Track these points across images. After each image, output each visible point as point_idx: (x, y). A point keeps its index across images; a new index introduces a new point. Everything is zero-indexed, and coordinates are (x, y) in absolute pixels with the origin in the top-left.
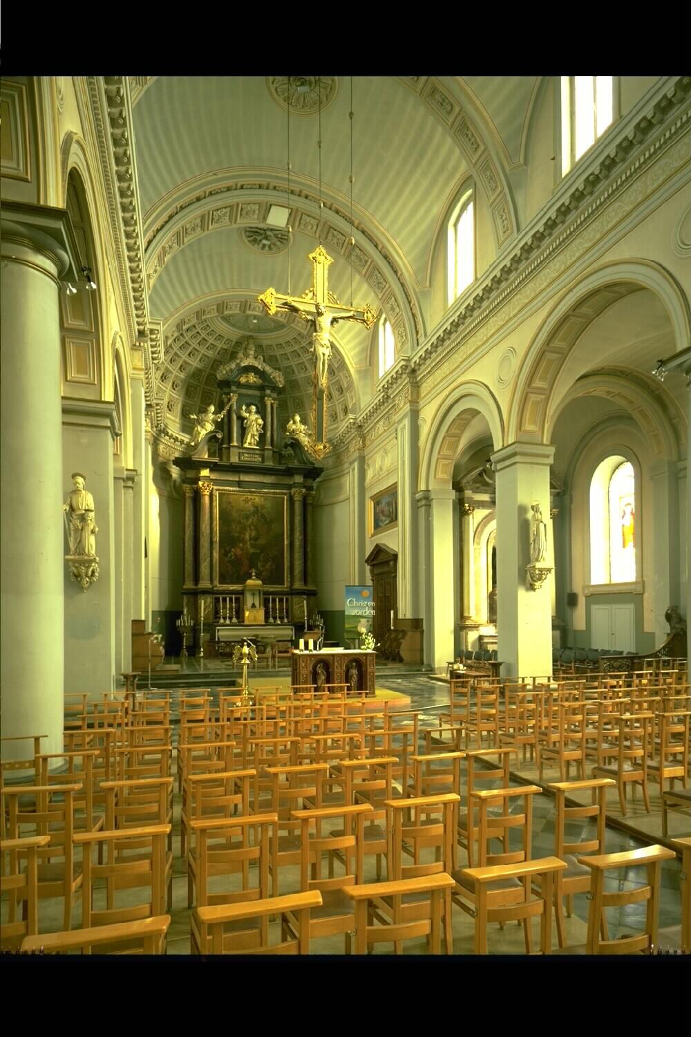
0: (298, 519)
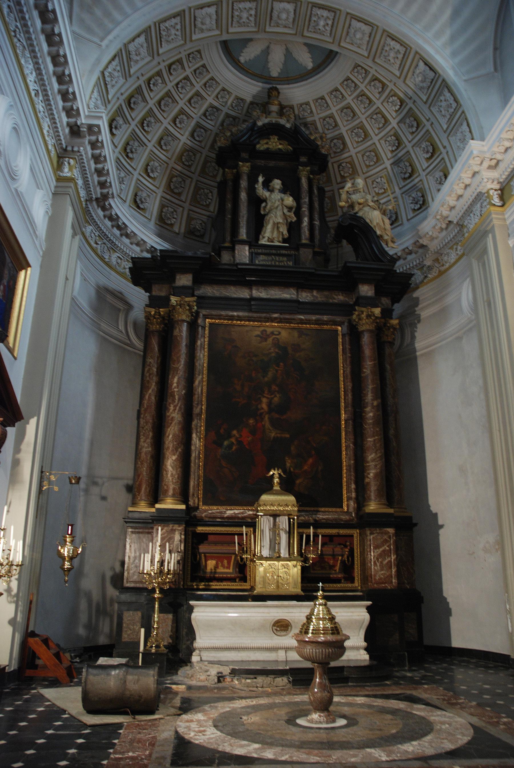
0: (368, 366)
